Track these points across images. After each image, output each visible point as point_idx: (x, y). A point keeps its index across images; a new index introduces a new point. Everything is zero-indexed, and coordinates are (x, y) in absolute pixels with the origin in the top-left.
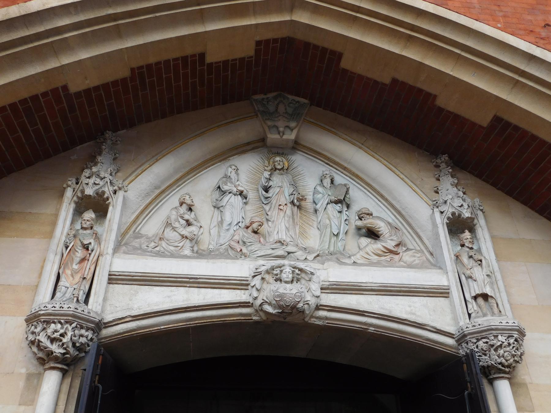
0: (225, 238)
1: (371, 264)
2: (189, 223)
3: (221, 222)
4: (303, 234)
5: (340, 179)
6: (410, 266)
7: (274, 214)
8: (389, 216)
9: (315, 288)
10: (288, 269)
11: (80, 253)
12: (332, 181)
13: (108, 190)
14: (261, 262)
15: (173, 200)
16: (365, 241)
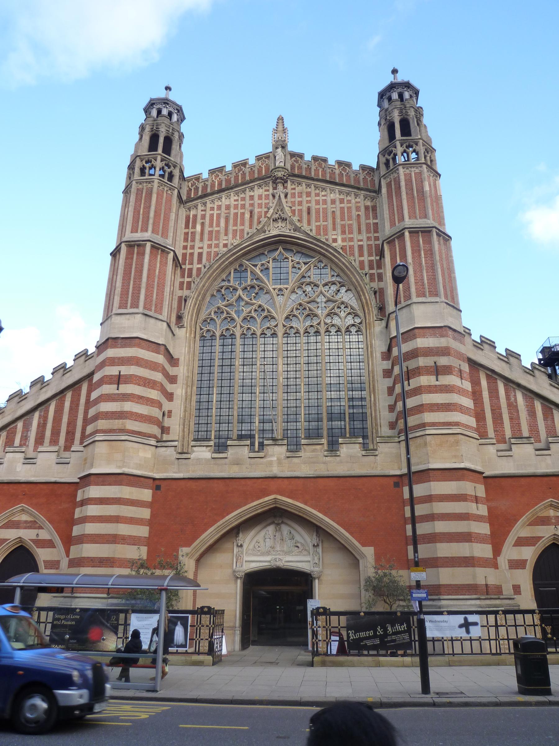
0: (267, 548)
1: (297, 555)
2: (259, 547)
3: (265, 545)
4: (283, 547)
5: (293, 531)
6: (304, 555)
7: (276, 543)
8: (303, 541)
9: (283, 562)
10: (277, 559)
11: (240, 557)
12: (290, 533)
13: (242, 543)
14: (273, 556)
15: (255, 540)
16: (296, 548)
